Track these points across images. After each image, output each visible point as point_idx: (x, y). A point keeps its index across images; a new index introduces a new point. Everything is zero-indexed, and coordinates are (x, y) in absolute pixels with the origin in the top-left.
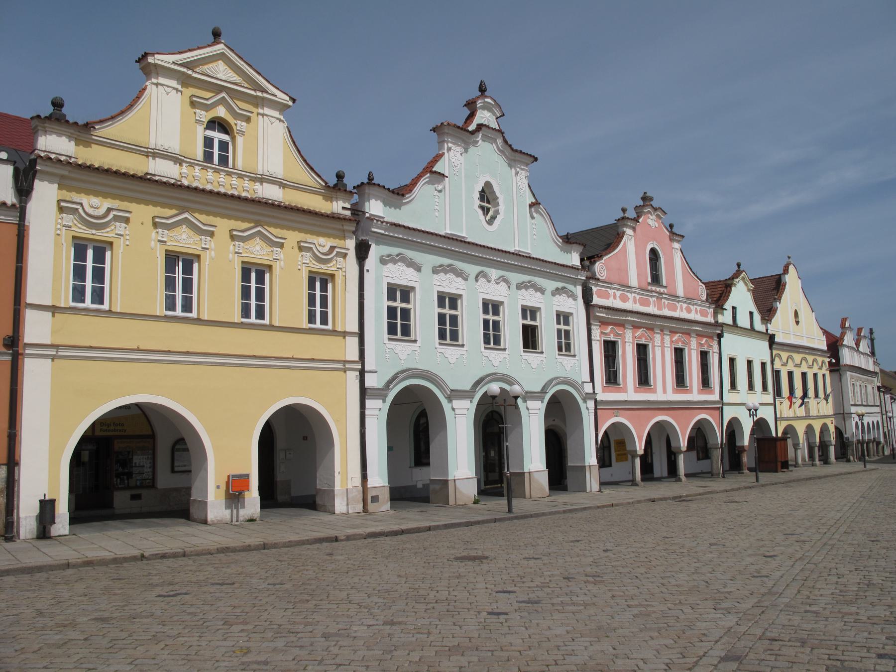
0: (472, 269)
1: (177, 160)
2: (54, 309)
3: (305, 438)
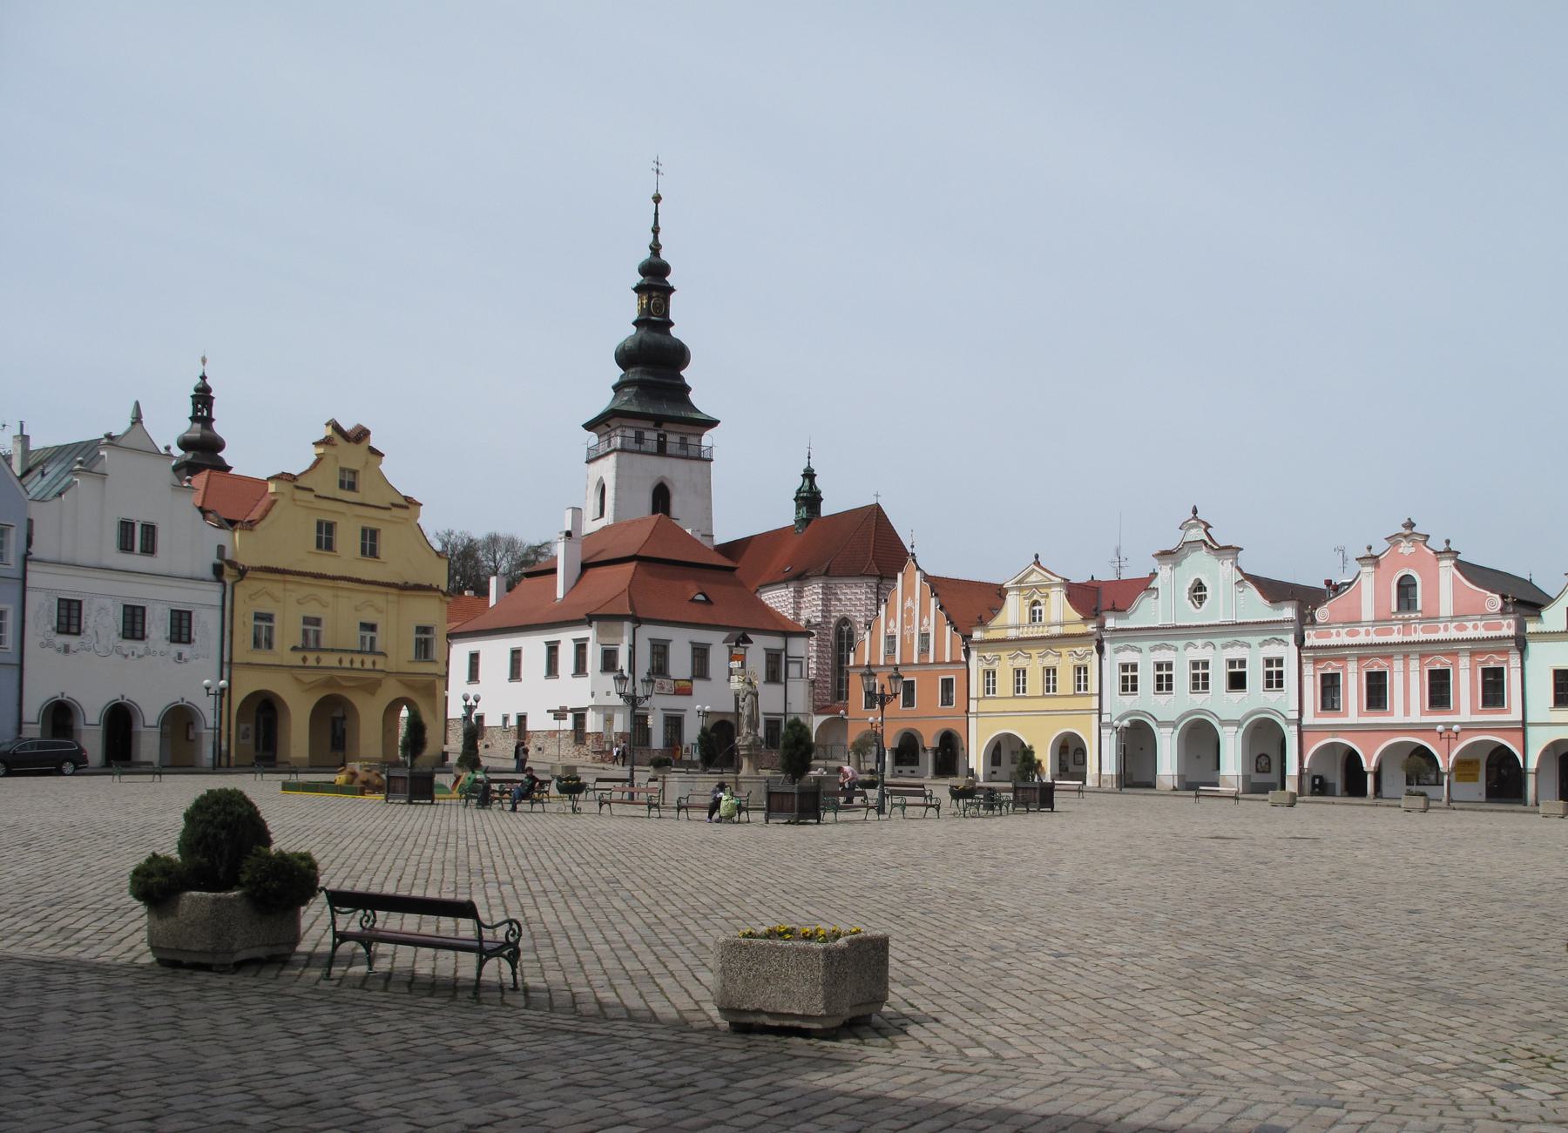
0: (1180, 644)
1: (1017, 627)
2: (978, 699)
3: (1198, 757)
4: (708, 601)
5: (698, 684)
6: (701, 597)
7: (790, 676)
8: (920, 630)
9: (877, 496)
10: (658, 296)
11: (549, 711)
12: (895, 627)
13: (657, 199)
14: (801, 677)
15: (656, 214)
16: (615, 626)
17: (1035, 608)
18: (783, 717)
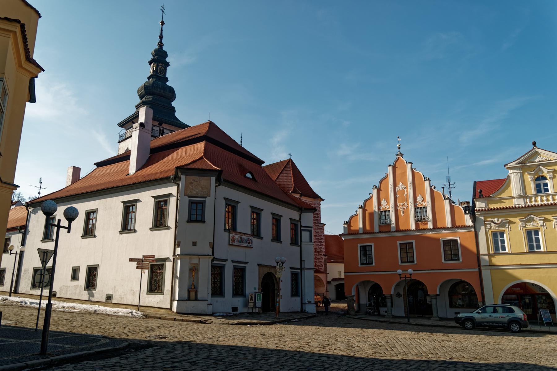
4: (254, 179)
5: (255, 240)
6: (249, 175)
7: (303, 241)
8: (415, 206)
9: (290, 155)
10: (161, 66)
11: (131, 260)
12: (388, 204)
13: (163, 23)
14: (311, 241)
15: (162, 30)
16: (203, 181)
17: (538, 182)
18: (299, 271)
